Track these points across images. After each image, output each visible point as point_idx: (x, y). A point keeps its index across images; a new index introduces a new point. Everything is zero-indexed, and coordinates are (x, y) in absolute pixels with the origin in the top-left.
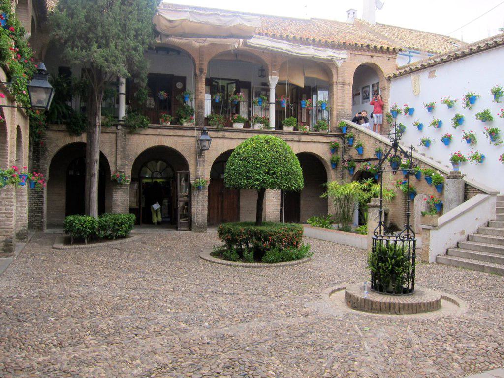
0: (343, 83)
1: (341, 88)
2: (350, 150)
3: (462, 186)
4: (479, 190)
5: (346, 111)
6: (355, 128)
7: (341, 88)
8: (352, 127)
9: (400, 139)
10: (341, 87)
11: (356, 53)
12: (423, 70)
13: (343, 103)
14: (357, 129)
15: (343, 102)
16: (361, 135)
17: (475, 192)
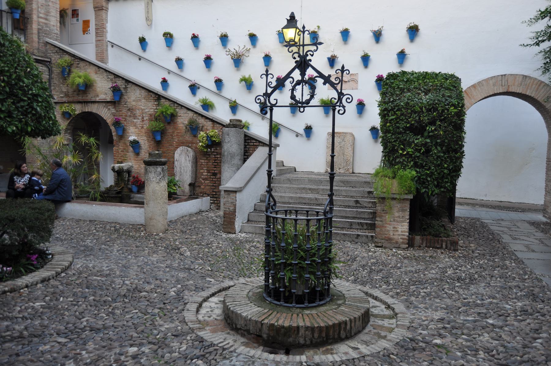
3: (243, 136)
4: (260, 142)
9: (312, 55)
13: (47, 15)
15: (47, 13)
16: (82, 64)
17: (255, 144)
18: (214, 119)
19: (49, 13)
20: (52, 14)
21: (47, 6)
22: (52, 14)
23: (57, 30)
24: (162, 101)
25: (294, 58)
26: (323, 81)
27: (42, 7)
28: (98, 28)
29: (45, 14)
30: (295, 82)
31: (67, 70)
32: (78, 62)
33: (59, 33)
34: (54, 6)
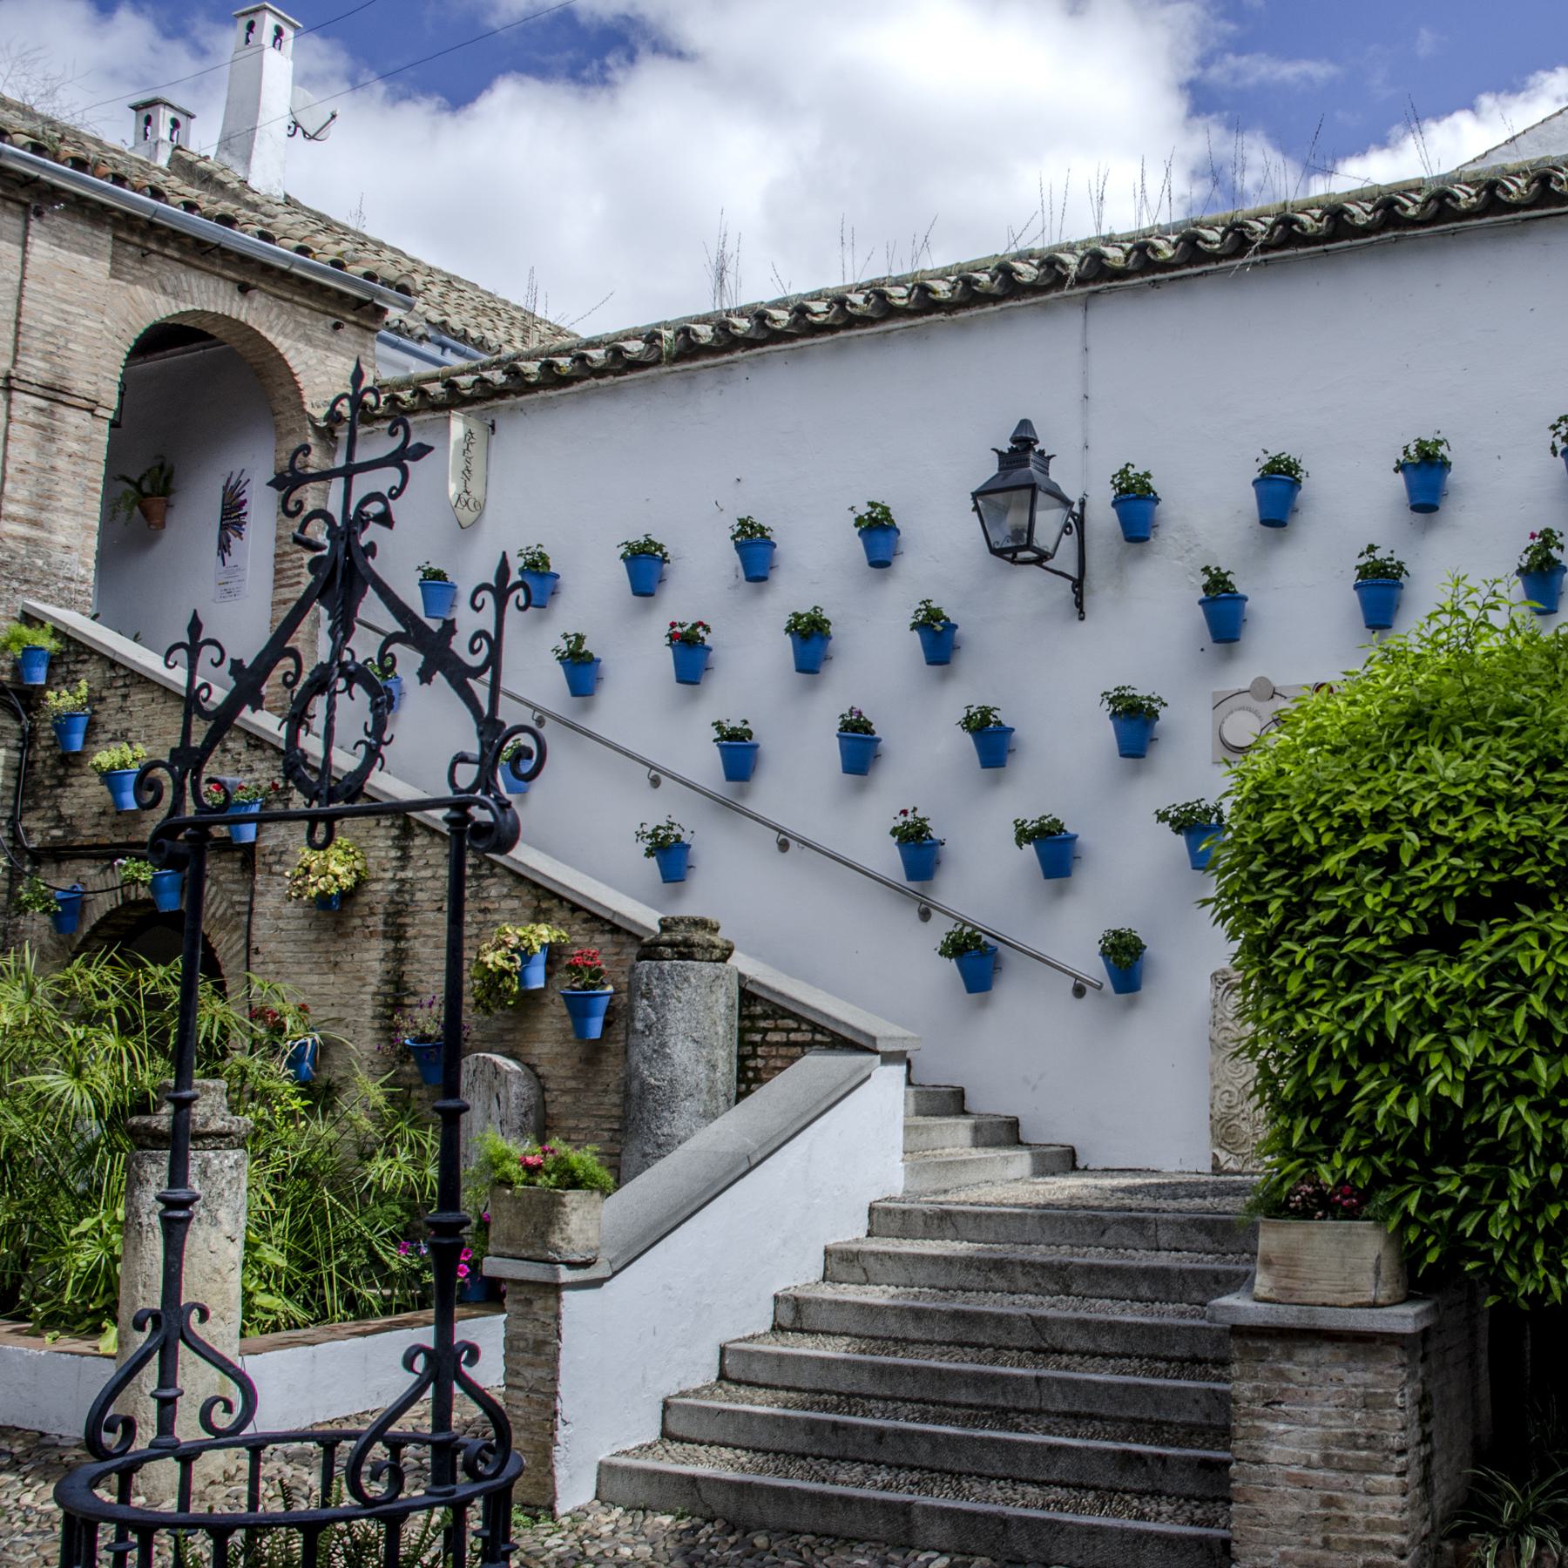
0: (55, 393)
1: (32, 417)
2: (62, 783)
5: (57, 556)
6: (102, 657)
7: (32, 417)
8: (92, 652)
10: (41, 410)
11: (153, 246)
12: (511, 400)
14: (113, 664)
16: (138, 697)
18: (616, 921)
19: (49, 498)
20: (66, 502)
21: (43, 470)
22: (66, 502)
23: (84, 564)
24: (418, 841)
25: (312, 546)
26: (418, 659)
27: (20, 476)
28: (285, 554)
29: (32, 504)
30: (305, 677)
31: (81, 723)
32: (123, 691)
33: (91, 576)
34: (78, 469)
